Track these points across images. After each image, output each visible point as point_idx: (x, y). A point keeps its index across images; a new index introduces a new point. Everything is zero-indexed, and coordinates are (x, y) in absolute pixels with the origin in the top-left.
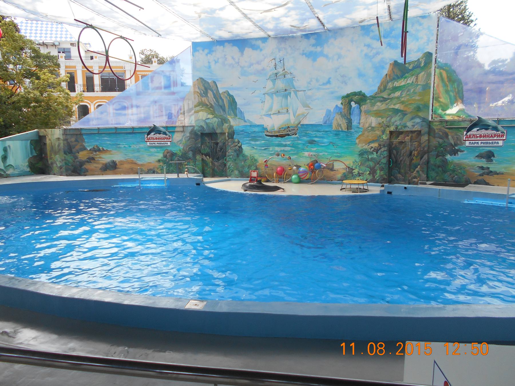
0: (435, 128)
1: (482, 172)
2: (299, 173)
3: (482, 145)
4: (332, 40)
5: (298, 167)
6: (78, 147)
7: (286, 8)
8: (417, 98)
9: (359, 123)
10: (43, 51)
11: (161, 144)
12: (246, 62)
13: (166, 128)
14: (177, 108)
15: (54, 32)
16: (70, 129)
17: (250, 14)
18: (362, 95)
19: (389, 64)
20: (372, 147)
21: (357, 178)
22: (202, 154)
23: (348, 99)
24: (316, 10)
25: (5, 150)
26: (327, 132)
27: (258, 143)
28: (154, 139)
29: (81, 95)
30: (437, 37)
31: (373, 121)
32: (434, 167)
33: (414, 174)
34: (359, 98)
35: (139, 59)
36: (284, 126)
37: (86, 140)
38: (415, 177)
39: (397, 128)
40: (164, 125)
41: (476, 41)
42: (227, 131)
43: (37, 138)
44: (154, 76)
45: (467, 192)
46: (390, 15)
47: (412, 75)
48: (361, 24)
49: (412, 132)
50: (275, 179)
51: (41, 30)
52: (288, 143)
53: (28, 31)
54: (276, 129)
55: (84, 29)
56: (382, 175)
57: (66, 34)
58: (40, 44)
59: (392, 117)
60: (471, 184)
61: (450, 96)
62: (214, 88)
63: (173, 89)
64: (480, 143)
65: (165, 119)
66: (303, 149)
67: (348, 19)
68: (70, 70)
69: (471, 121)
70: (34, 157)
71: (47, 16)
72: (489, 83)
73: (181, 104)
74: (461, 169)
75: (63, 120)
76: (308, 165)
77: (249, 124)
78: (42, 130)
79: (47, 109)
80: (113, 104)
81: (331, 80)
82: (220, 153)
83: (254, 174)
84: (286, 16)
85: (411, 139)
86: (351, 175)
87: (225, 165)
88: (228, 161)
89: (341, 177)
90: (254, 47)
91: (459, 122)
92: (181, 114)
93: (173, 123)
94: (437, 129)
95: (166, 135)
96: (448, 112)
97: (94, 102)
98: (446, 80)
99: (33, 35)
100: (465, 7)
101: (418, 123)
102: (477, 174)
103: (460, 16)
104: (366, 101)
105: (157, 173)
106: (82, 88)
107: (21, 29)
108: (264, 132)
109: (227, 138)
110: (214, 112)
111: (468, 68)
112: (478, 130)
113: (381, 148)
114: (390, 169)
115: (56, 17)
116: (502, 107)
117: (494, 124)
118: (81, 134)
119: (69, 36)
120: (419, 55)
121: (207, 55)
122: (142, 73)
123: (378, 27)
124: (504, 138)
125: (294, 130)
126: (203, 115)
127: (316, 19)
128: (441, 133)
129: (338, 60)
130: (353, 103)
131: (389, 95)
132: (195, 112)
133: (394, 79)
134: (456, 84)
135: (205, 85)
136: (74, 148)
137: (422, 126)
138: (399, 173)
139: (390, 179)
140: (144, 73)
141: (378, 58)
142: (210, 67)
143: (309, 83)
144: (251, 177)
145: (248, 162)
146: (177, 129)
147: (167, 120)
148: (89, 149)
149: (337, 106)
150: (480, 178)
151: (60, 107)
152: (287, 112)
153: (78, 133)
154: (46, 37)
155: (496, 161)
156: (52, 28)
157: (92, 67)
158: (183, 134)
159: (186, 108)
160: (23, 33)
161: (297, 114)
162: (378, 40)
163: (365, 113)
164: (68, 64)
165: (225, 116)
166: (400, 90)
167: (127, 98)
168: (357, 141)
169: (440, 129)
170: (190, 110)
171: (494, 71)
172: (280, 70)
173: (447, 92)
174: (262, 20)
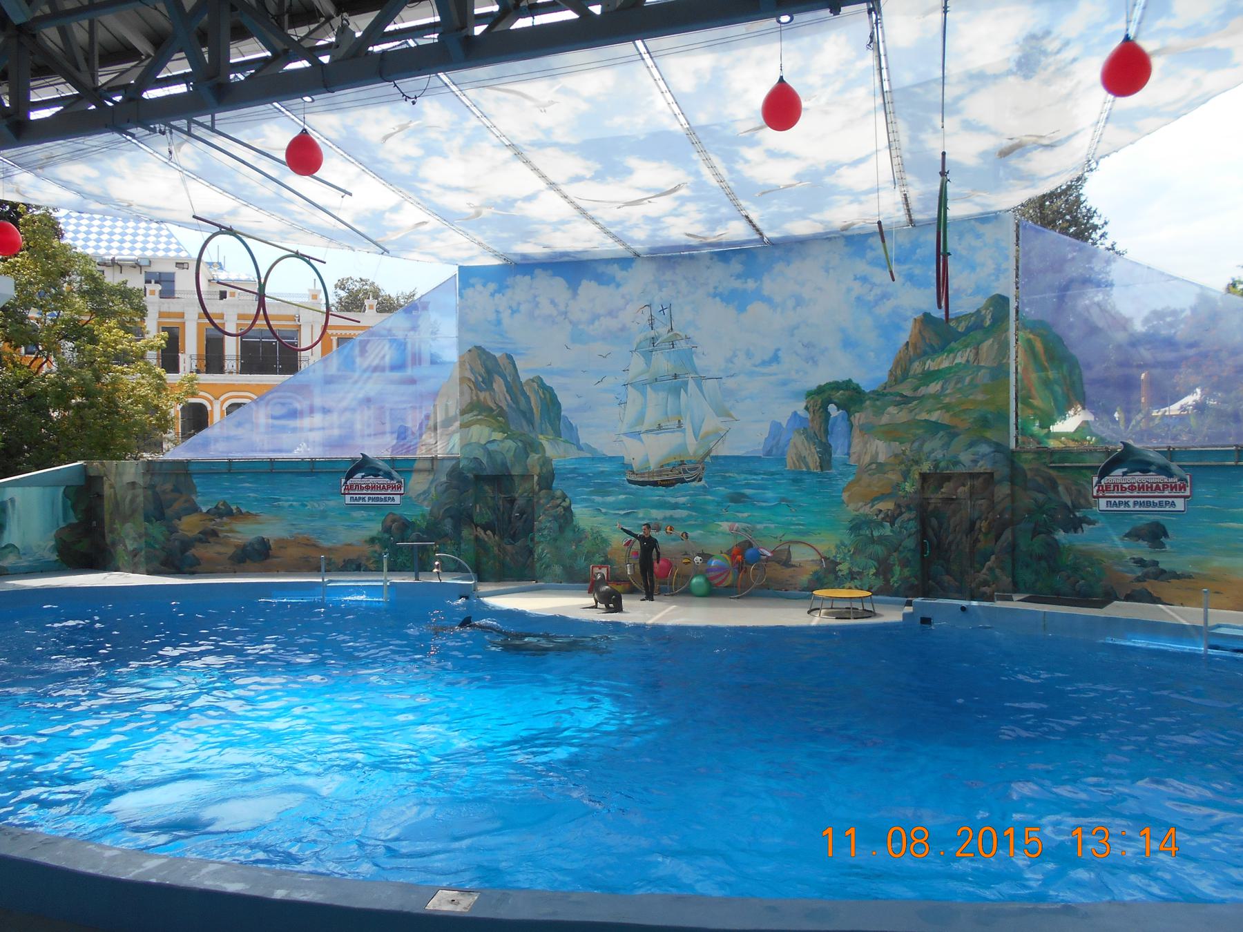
0: (1026, 467)
1: (1139, 572)
2: (709, 570)
3: (1137, 508)
4: (779, 267)
5: (706, 557)
8: (980, 397)
9: (848, 454)
10: (112, 278)
11: (378, 499)
13: (392, 461)
14: (420, 416)
15: (140, 238)
17: (595, 209)
21: (847, 585)
22: (476, 526)
23: (821, 397)
24: (743, 203)
26: (772, 474)
27: (611, 499)
28: (362, 489)
31: (881, 449)
33: (983, 574)
34: (849, 396)
35: (333, 300)
37: (198, 489)
38: (985, 583)
39: (936, 467)
40: (387, 455)
44: (368, 341)
45: (1110, 622)
47: (966, 347)
49: (973, 476)
51: (111, 234)
52: (682, 500)
57: (168, 243)
58: (104, 264)
59: (924, 441)
61: (1053, 392)
62: (508, 371)
63: (409, 372)
65: (390, 440)
66: (718, 515)
69: (1108, 453)
70: (71, 527)
71: (130, 205)
72: (1142, 367)
73: (428, 408)
76: (728, 553)
77: (589, 455)
78: (96, 463)
79: (109, 413)
80: (267, 404)
81: (780, 354)
82: (519, 524)
84: (675, 213)
85: (972, 493)
86: (831, 577)
87: (531, 552)
88: (539, 542)
90: (603, 280)
91: (1081, 453)
94: (1030, 470)
95: (392, 479)
96: (1055, 428)
97: (222, 398)
98: (1043, 358)
99: (92, 243)
100: (1078, 197)
101: (984, 456)
104: (862, 402)
105: (367, 570)
106: (195, 363)
107: (67, 231)
108: (625, 474)
109: (537, 488)
111: (1093, 330)
112: (1124, 474)
113: (901, 514)
115: (150, 208)
116: (1180, 418)
117: (1162, 460)
118: (188, 474)
119: (173, 247)
120: (979, 301)
121: (492, 295)
122: (339, 332)
123: (883, 241)
124: (1188, 493)
126: (481, 433)
129: (794, 308)
130: (832, 408)
131: (916, 389)
132: (462, 426)
133: (925, 353)
134: (1065, 368)
138: (948, 572)
139: (925, 585)
140: (343, 332)
142: (499, 322)
143: (730, 360)
145: (587, 545)
147: (395, 442)
148: (204, 510)
149: (795, 413)
150: (1138, 586)
153: (182, 470)
154: (120, 249)
155: (1172, 547)
156: (136, 228)
157: (222, 316)
158: (431, 477)
160: (67, 240)
164: (165, 309)
165: (532, 435)
167: (304, 389)
168: (845, 496)
170: (448, 422)
171: (1150, 340)
172: (662, 330)
173: (1047, 383)
174: (621, 222)
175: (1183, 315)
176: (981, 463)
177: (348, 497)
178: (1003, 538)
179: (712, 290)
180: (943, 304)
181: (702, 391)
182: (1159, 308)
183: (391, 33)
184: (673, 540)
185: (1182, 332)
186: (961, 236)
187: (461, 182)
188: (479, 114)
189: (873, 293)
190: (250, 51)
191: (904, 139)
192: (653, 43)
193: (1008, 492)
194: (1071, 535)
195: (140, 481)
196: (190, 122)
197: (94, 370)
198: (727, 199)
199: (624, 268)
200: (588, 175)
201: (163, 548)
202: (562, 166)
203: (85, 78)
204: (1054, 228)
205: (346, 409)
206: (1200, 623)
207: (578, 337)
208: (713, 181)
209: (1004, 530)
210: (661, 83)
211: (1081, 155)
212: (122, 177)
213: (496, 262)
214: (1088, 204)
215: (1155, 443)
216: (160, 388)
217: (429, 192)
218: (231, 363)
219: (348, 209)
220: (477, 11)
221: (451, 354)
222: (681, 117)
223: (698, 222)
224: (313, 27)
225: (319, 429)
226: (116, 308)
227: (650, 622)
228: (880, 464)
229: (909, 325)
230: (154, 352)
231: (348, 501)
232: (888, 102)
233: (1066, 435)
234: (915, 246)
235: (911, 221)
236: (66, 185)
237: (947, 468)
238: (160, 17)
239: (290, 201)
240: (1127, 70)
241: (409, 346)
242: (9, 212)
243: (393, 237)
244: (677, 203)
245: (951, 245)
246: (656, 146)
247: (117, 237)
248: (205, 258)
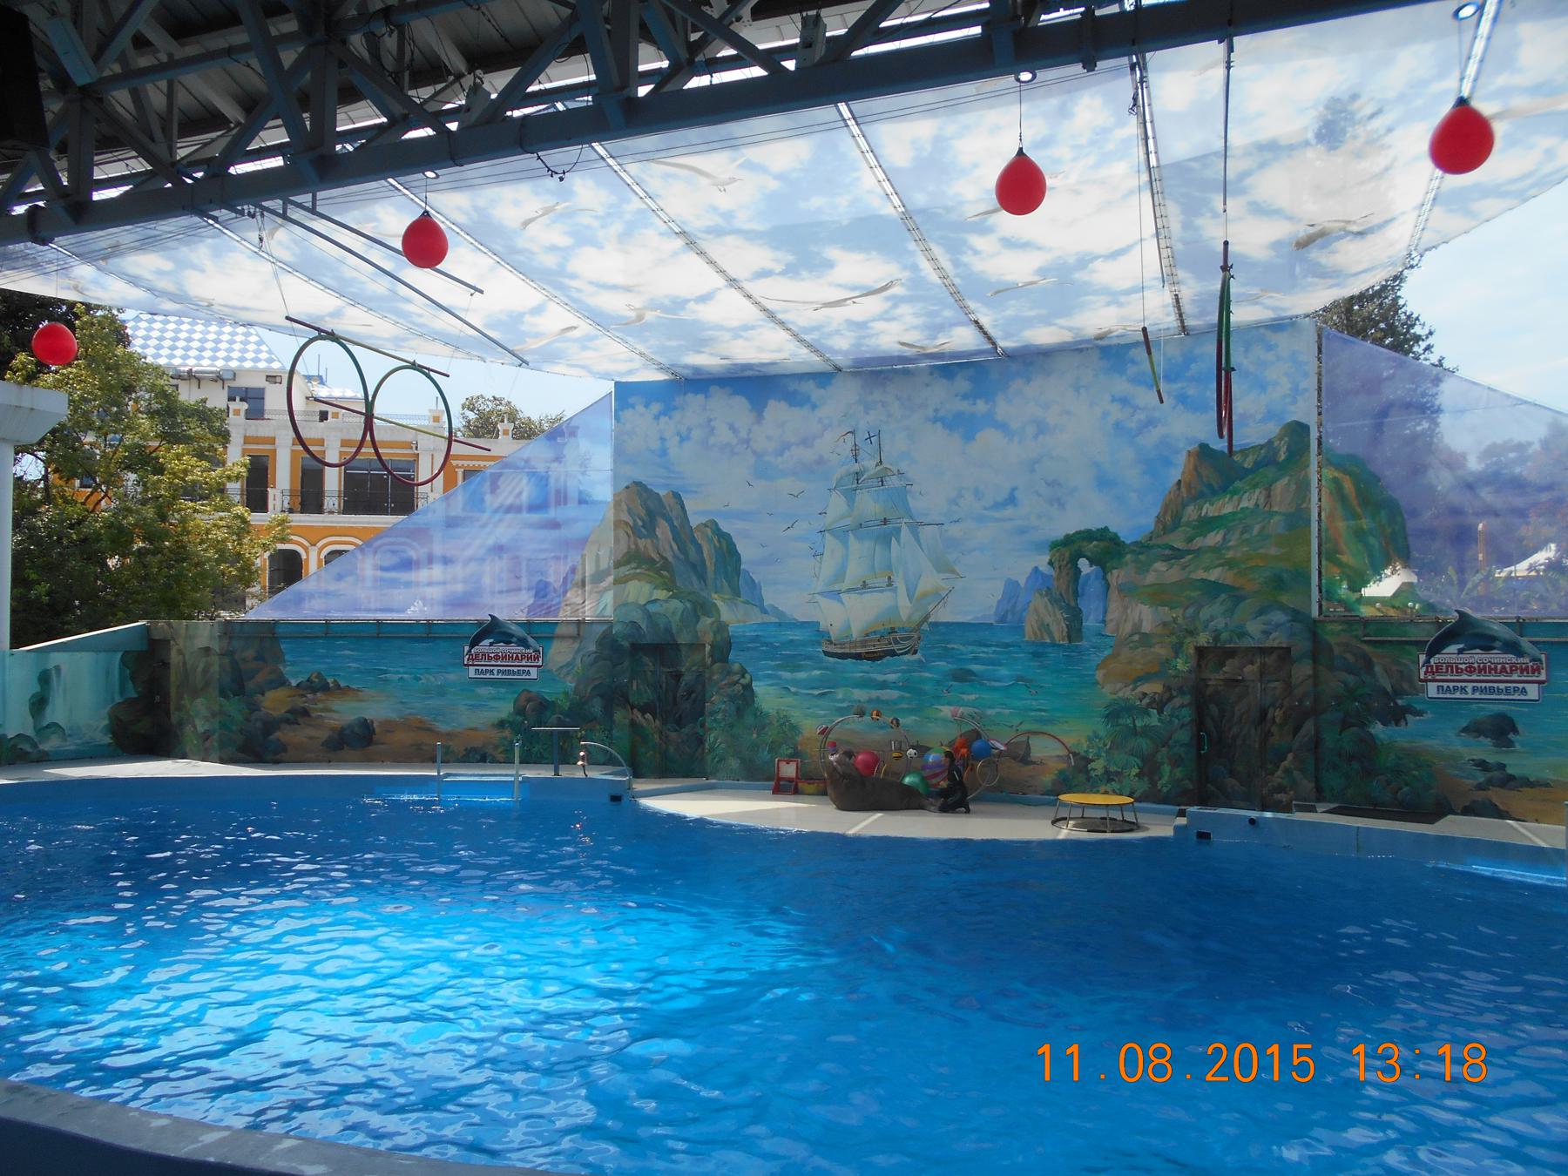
0: (1332, 640)
1: (1481, 777)
2: (924, 768)
3: (1477, 695)
5: (922, 750)
7: (887, 299)
8: (1273, 551)
10: (188, 395)
12: (769, 438)
13: (528, 625)
14: (564, 569)
15: (223, 346)
17: (786, 311)
19: (1185, 453)
20: (1145, 695)
21: (1102, 788)
23: (1070, 549)
24: (972, 305)
25: (45, 679)
26: (1007, 645)
27: (802, 675)
28: (490, 659)
30: (1319, 381)
31: (1146, 616)
33: (1278, 777)
34: (1102, 547)
36: (881, 628)
37: (287, 657)
39: (1216, 639)
40: (523, 617)
44: (500, 475)
45: (1445, 842)
47: (1255, 486)
48: (1100, 343)
51: (189, 340)
52: (892, 677)
53: (153, 342)
54: (856, 634)
57: (258, 352)
58: (179, 377)
59: (1202, 606)
64: (1469, 690)
65: (527, 598)
66: (937, 697)
67: (1062, 327)
69: (1439, 624)
70: (129, 703)
73: (574, 558)
78: (161, 623)
80: (375, 553)
81: (1017, 494)
83: (789, 770)
84: (885, 317)
85: (1262, 673)
86: (1082, 777)
87: (700, 741)
91: (1402, 624)
93: (547, 614)
95: (528, 647)
96: (1371, 591)
97: (320, 544)
101: (1278, 625)
104: (1120, 555)
105: (495, 761)
106: (287, 500)
108: (820, 644)
109: (709, 661)
112: (1460, 651)
113: (1171, 698)
115: (233, 308)
117: (1508, 634)
119: (264, 356)
120: (1272, 429)
121: (657, 417)
122: (466, 463)
123: (1149, 353)
124: (1543, 677)
125: (909, 638)
126: (640, 591)
127: (973, 327)
128: (1349, 656)
129: (1036, 437)
130: (1083, 564)
131: (1190, 540)
132: (616, 582)
134: (1383, 513)
138: (1232, 773)
139: (1202, 789)
140: (471, 463)
141: (1155, 434)
142: (664, 453)
144: (780, 779)
146: (559, 630)
148: (294, 683)
149: (1036, 568)
152: (890, 585)
153: (268, 632)
156: (219, 333)
157: (321, 442)
158: (576, 646)
159: (590, 570)
160: (136, 346)
162: (1150, 387)
163: (1120, 591)
165: (704, 594)
167: (421, 534)
168: (1099, 675)
170: (599, 577)
172: (869, 464)
173: (1359, 535)
174: (817, 328)
175: (1530, 451)
177: (472, 669)
178: (1303, 732)
180: (1225, 432)
181: (918, 540)
182: (1499, 441)
183: (533, 93)
184: (881, 728)
186: (1248, 347)
187: (619, 279)
188: (642, 194)
189: (1136, 417)
190: (362, 117)
191: (1175, 225)
192: (860, 106)
195: (216, 646)
196: (287, 202)
198: (951, 300)
199: (822, 385)
200: (778, 269)
201: (241, 731)
202: (745, 258)
203: (160, 149)
204: (1364, 338)
205: (471, 559)
207: (763, 471)
208: (934, 277)
210: (870, 156)
211: (1400, 249)
212: (203, 271)
213: (661, 377)
214: (1408, 309)
215: (1496, 612)
216: (242, 529)
217: (578, 290)
218: (331, 502)
219: (479, 310)
220: (641, 68)
221: (604, 492)
222: (895, 198)
223: (915, 328)
224: (439, 87)
225: (438, 583)
226: (192, 433)
227: (851, 832)
229: (1181, 459)
230: (238, 485)
231: (472, 674)
232: (1156, 180)
233: (1382, 600)
235: (1184, 328)
236: (134, 281)
238: (251, 73)
239: (407, 300)
240: (1462, 141)
241: (552, 481)
242: (66, 314)
243: (534, 345)
244: (889, 304)
245: (1237, 357)
246: (864, 233)
247: (196, 344)
248: (297, 368)
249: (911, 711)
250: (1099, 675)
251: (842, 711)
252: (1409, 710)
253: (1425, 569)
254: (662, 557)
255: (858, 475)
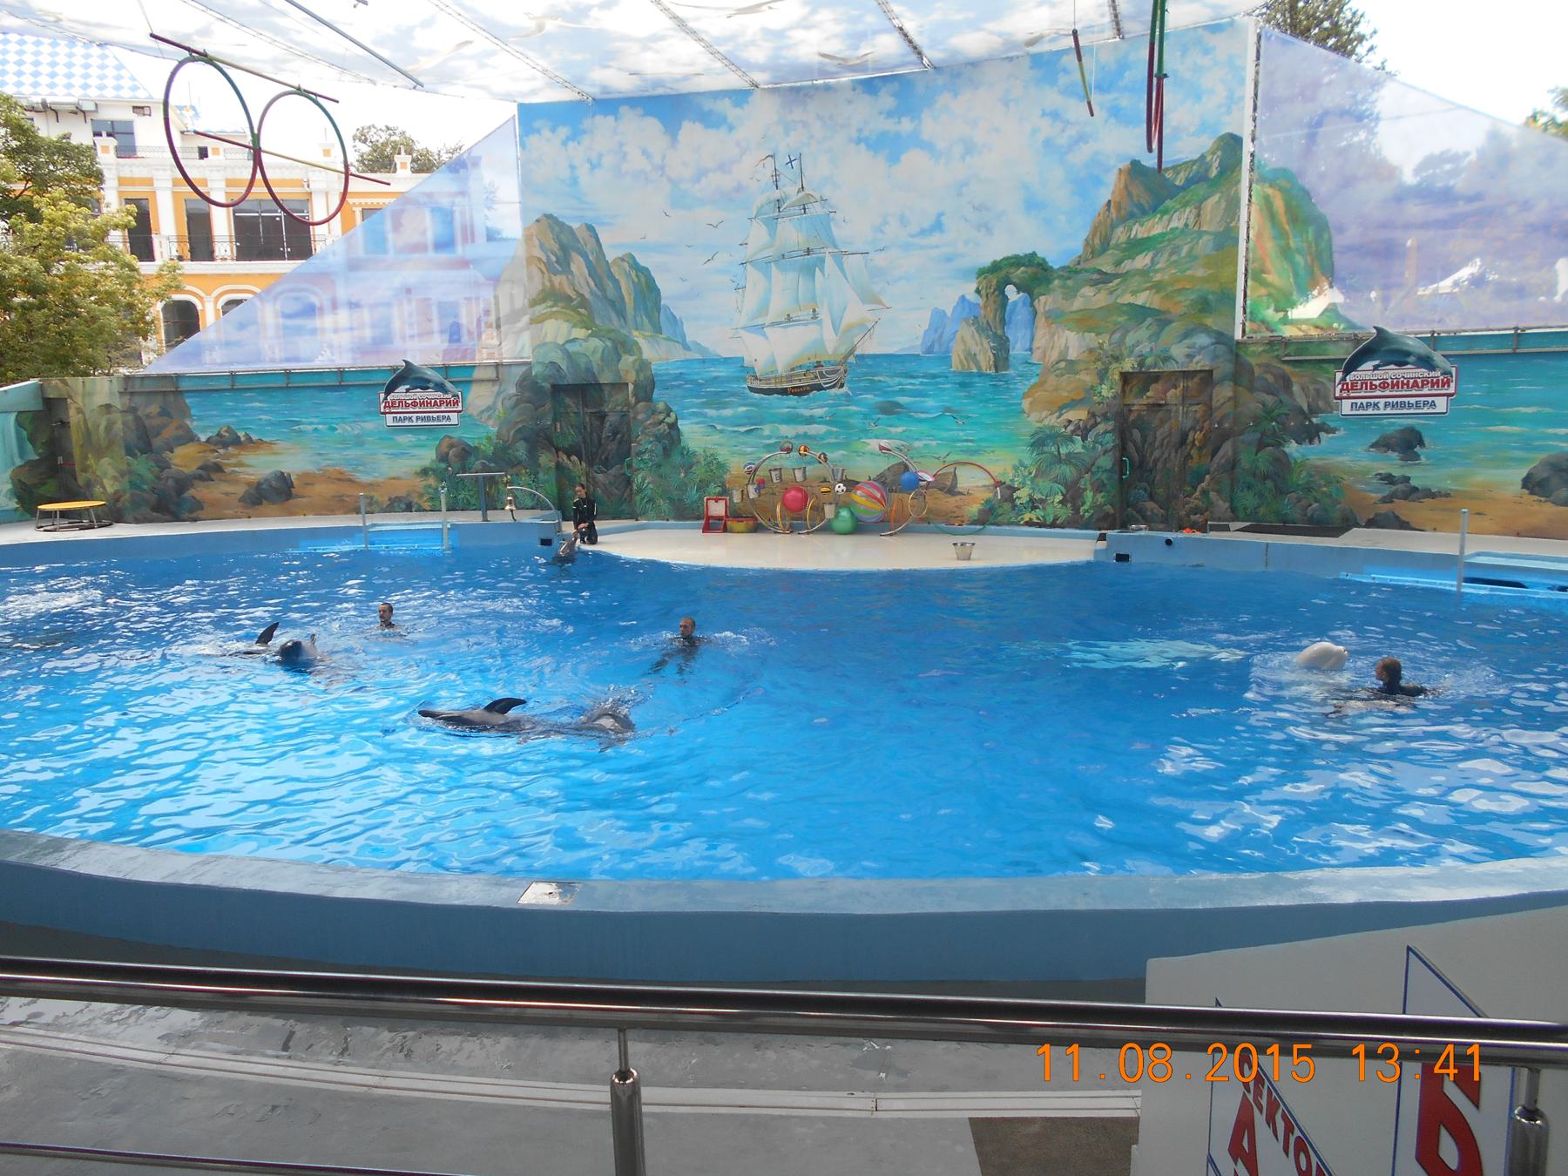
0: (1253, 361)
1: (1388, 490)
3: (1388, 411)
6: (169, 432)
8: (1200, 273)
9: (1030, 349)
11: (428, 419)
16: (144, 378)
17: (697, 19)
18: (1039, 265)
19: (1116, 171)
23: (997, 277)
24: (896, 8)
26: (934, 376)
27: (728, 412)
28: (407, 405)
29: (175, 269)
31: (1073, 343)
32: (1250, 479)
33: (1195, 500)
34: (1031, 274)
35: (353, 158)
36: (806, 362)
37: (193, 412)
38: (1196, 510)
39: (1141, 364)
40: (439, 361)
41: (1374, 96)
42: (631, 378)
43: (39, 407)
44: (403, 211)
46: (1118, 24)
47: (1185, 205)
49: (1187, 375)
50: (779, 521)
52: (818, 412)
54: (781, 369)
55: (181, 64)
56: (1101, 506)
59: (1127, 331)
60: (1358, 526)
61: (1293, 264)
62: (590, 247)
64: (1381, 406)
66: (865, 431)
67: (991, 33)
68: (137, 191)
69: (1356, 340)
70: (31, 465)
71: (58, 20)
72: (1408, 226)
74: (1328, 483)
75: (117, 349)
78: (55, 381)
79: (66, 316)
80: (275, 298)
81: (943, 219)
82: (613, 446)
83: (717, 509)
84: (805, 24)
85: (1184, 397)
86: (1007, 506)
87: (629, 482)
89: (980, 511)
90: (710, 120)
91: (1322, 342)
92: (490, 326)
93: (464, 358)
95: (446, 392)
96: (1294, 314)
98: (1282, 218)
101: (1202, 348)
102: (1376, 496)
103: (1326, 24)
104: (1049, 281)
105: (420, 510)
106: (174, 247)
108: (745, 380)
109: (633, 400)
110: (593, 322)
112: (1376, 368)
113: (1096, 424)
114: (1124, 486)
115: (86, 24)
117: (1423, 349)
118: (178, 393)
120: (1205, 143)
121: (564, 143)
122: (363, 201)
123: (1080, 59)
124: (1451, 390)
126: (558, 330)
127: (897, 34)
128: (1270, 378)
129: (963, 158)
130: (1010, 291)
131: (1118, 263)
132: (533, 321)
133: (1132, 216)
134: (1311, 230)
135: (562, 237)
136: (159, 434)
137: (1215, 357)
138: (1151, 497)
142: (574, 181)
144: (709, 518)
145: (699, 472)
147: (445, 345)
148: (203, 438)
149: (963, 297)
151: (107, 307)
152: (815, 317)
153: (170, 390)
158: (496, 389)
159: (505, 309)
161: (845, 322)
164: (126, 173)
166: (1148, 249)
168: (1026, 404)
169: (1267, 366)
170: (515, 316)
171: (1424, 193)
172: (790, 190)
173: (1286, 252)
174: (732, 38)
175: (1465, 163)
176: (1197, 358)
178: (1221, 453)
179: (854, 134)
180: (1155, 145)
185: (1459, 184)
186: (1185, 50)
193: (1230, 394)
194: (1306, 447)
195: (118, 403)
197: (42, 259)
201: (153, 490)
204: (1307, 39)
206: (1455, 551)
209: (1223, 442)
215: (1417, 328)
216: (130, 279)
221: (512, 225)
223: (836, 36)
228: (1071, 362)
233: (1306, 322)
234: (1123, 66)
237: (1155, 365)
241: (457, 216)
243: (426, 63)
248: (171, 101)
249: (838, 446)
250: (1026, 404)
251: (769, 448)
252: (1323, 428)
253: (1347, 290)
254: (582, 295)
255: (779, 202)
